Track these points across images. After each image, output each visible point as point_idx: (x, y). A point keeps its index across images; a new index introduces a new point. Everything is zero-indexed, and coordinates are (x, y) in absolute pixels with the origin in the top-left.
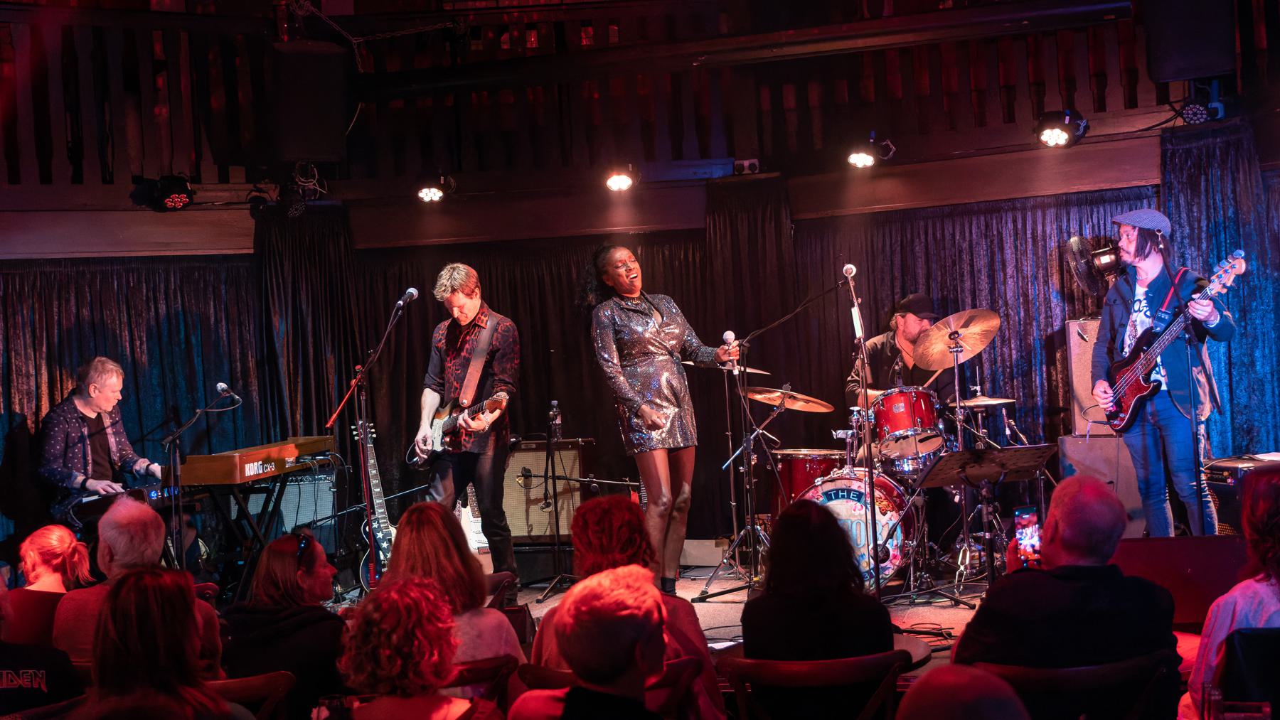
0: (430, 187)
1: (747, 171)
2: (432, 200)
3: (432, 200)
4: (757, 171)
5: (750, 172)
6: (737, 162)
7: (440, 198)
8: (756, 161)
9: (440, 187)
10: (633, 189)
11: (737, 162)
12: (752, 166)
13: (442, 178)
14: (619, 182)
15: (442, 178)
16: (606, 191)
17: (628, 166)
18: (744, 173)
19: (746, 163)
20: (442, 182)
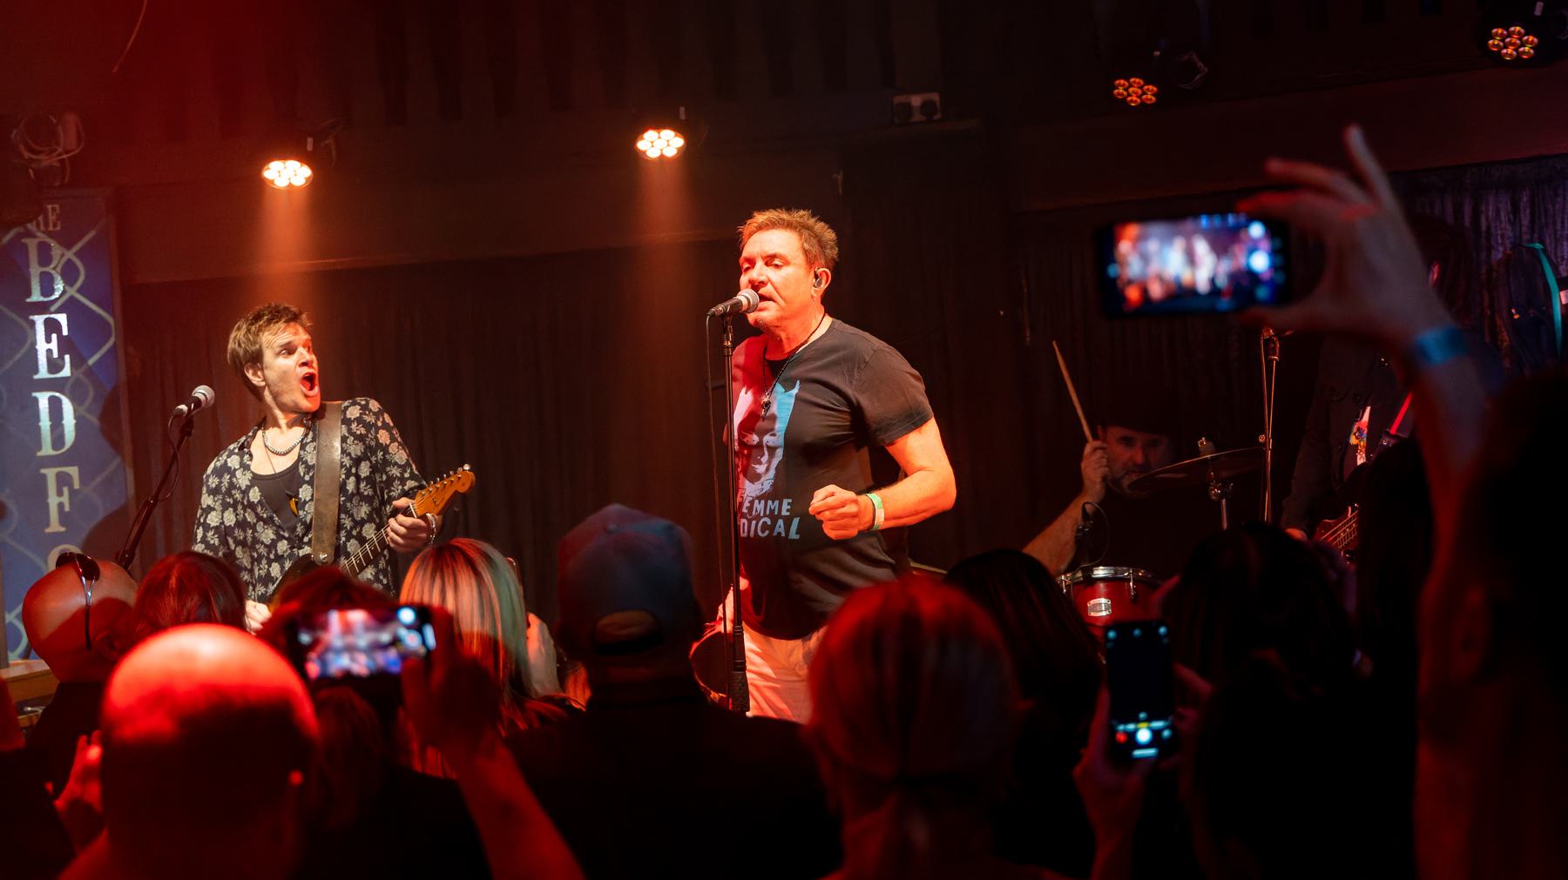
0: (284, 158)
1: (917, 117)
2: (290, 185)
3: (290, 185)
4: (938, 116)
5: (923, 118)
6: (898, 99)
7: (307, 179)
8: (935, 97)
9: (304, 158)
10: (685, 153)
11: (898, 99)
12: (927, 107)
13: (310, 140)
14: (661, 144)
15: (310, 140)
16: (638, 156)
17: (678, 112)
18: (912, 120)
19: (916, 101)
20: (310, 147)
